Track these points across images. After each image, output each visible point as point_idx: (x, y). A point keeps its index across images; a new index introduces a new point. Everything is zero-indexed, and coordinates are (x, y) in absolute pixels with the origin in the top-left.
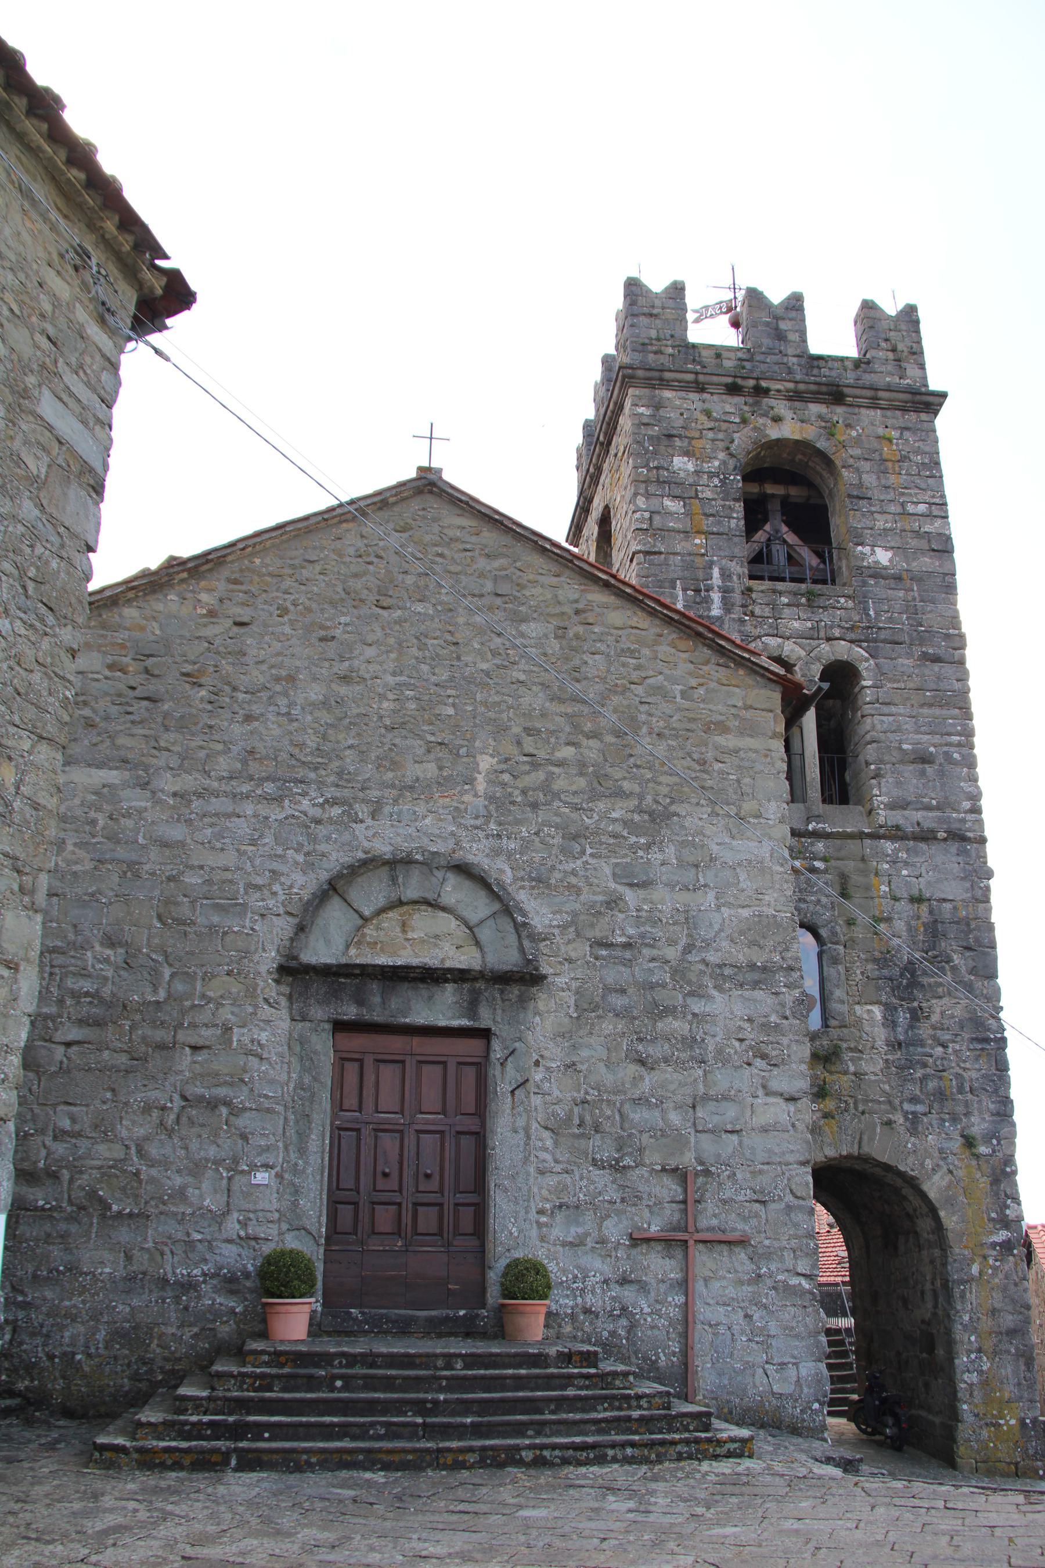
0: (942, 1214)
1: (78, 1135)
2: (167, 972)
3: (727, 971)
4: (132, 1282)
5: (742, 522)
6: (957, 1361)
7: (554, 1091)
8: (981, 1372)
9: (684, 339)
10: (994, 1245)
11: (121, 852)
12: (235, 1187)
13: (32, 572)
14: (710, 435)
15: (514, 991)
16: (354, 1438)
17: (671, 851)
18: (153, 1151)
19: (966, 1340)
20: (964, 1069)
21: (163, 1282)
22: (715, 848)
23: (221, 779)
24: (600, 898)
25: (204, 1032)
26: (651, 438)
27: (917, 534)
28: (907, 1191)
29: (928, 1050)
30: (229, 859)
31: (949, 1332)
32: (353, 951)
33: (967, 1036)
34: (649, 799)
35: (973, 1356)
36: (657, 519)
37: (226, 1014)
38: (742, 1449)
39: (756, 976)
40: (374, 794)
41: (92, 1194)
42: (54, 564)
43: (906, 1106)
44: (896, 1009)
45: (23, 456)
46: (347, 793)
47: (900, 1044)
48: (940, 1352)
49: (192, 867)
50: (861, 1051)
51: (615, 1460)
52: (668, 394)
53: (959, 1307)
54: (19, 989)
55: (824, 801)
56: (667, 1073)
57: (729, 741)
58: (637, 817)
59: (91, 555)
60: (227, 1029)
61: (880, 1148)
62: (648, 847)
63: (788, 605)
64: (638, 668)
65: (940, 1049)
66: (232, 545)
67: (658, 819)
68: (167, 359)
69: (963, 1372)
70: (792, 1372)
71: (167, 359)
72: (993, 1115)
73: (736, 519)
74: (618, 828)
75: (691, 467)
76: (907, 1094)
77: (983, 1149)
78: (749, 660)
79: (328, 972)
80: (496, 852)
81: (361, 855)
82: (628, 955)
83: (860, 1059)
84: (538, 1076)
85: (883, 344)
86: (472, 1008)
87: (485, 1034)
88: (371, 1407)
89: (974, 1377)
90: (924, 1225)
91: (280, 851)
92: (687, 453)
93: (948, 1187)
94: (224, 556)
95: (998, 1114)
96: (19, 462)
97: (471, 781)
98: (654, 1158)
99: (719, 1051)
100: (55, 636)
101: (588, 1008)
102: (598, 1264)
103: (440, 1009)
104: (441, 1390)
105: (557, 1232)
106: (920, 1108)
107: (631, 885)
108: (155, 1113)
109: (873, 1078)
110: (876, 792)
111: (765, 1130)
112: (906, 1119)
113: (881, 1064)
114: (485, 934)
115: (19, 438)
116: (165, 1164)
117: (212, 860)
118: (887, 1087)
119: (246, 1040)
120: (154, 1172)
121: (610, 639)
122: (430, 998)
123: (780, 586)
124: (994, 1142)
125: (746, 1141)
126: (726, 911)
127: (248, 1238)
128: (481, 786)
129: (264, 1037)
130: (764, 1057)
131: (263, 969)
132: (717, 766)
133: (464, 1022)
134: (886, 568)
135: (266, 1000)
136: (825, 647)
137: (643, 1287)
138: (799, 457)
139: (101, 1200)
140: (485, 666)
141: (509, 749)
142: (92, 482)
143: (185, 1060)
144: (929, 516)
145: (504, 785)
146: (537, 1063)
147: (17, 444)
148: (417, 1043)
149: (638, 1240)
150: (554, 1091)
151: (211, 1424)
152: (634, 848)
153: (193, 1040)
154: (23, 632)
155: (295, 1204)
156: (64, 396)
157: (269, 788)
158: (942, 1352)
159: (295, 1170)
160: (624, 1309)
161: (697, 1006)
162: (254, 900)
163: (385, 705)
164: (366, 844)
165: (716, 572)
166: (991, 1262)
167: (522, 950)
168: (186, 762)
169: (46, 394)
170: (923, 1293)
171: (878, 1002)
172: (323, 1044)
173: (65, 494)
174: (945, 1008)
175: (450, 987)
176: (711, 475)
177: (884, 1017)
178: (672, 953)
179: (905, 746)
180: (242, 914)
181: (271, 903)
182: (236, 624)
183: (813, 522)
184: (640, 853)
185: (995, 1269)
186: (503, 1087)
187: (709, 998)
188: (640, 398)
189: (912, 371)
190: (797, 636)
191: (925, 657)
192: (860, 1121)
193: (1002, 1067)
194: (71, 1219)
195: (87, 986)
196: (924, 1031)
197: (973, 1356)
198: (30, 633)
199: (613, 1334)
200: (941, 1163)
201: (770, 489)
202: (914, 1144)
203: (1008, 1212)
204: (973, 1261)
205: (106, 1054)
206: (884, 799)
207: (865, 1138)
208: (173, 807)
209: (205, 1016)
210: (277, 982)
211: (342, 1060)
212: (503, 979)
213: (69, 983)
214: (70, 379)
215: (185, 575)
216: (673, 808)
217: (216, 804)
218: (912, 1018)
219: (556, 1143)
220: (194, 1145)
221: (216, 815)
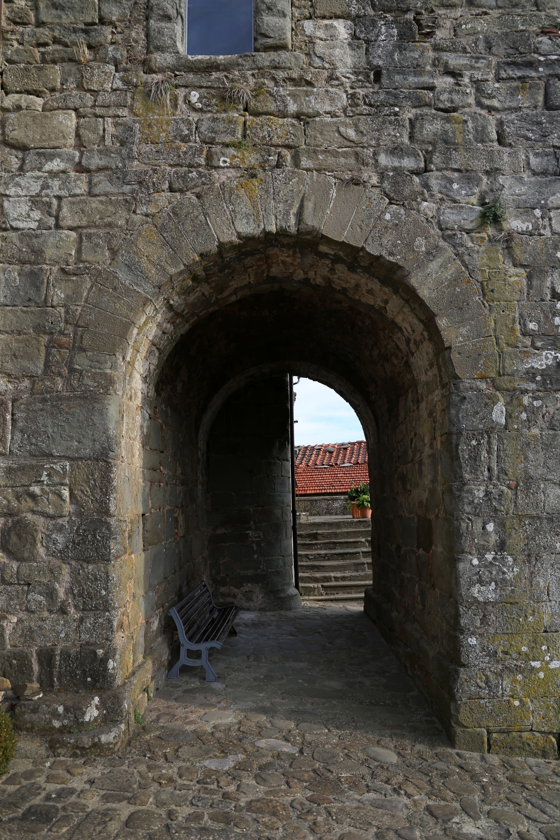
0: (442, 322)
8: (501, 583)
20: (490, 109)
29: (426, 79)
31: (452, 518)
33: (494, 60)
35: (489, 557)
43: (383, 160)
44: (374, 23)
47: (378, 75)
48: (439, 548)
50: (309, 84)
53: (467, 476)
65: (450, 80)
69: (471, 584)
72: (535, 173)
76: (385, 141)
83: (307, 94)
95: (544, 173)
106: (408, 163)
109: (328, 119)
112: (382, 176)
113: (344, 100)
118: (351, 133)
158: (440, 549)
166: (526, 400)
170: (421, 463)
177: (354, 36)
185: (532, 411)
192: (301, 181)
197: (489, 557)
200: (442, 243)
202: (395, 215)
207: (309, 206)
218: (401, 36)
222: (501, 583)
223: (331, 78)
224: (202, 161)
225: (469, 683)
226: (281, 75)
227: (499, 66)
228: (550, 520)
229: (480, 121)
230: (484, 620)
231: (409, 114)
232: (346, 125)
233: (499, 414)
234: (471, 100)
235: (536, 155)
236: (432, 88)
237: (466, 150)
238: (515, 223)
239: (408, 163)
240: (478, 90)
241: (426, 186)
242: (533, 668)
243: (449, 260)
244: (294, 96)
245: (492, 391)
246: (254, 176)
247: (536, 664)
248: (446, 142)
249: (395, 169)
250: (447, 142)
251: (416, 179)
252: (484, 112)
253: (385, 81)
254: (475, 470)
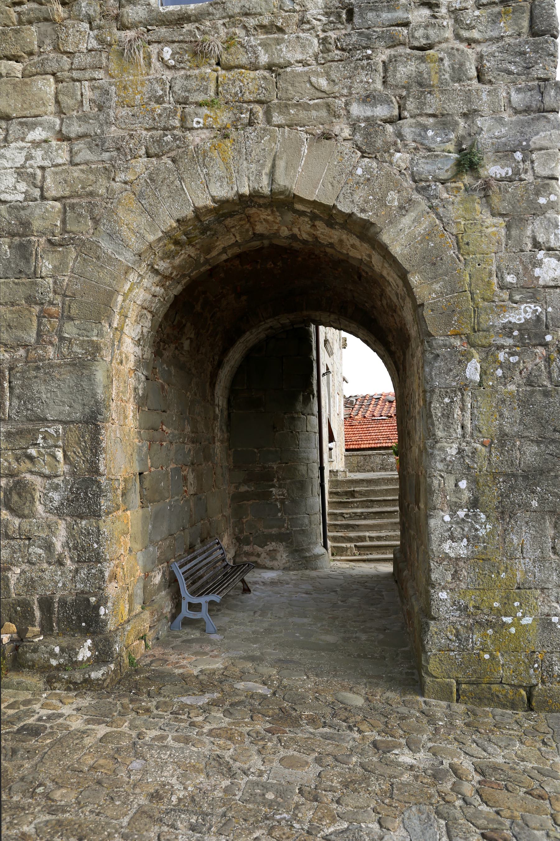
0: (415, 279)
6: (432, 522)
8: (473, 540)
10: (508, 330)
20: (470, 42)
29: (400, 15)
35: (461, 514)
43: (356, 110)
50: (280, 30)
53: (440, 434)
65: (426, 12)
69: (443, 540)
72: (517, 112)
76: (358, 89)
77: (494, 170)
83: (278, 42)
89: (461, 549)
95: (527, 110)
106: (381, 111)
109: (299, 69)
112: (354, 127)
118: (323, 83)
124: (518, 156)
192: (273, 139)
197: (461, 514)
200: (416, 196)
202: (367, 170)
203: (537, 272)
204: (468, 357)
207: (281, 164)
223: (302, 21)
224: (177, 123)
226: (252, 22)
228: (526, 477)
229: (458, 56)
230: (455, 575)
231: (383, 55)
232: (318, 75)
233: (473, 370)
234: (449, 34)
235: (519, 90)
236: (406, 24)
237: (442, 92)
238: (494, 170)
239: (381, 111)
240: (457, 21)
241: (400, 135)
242: (504, 623)
243: (423, 214)
244: (264, 44)
245: (466, 347)
246: (226, 136)
247: (508, 620)
248: (421, 85)
249: (367, 119)
250: (422, 83)
251: (390, 128)
252: (463, 46)
253: (357, 20)
254: (447, 427)
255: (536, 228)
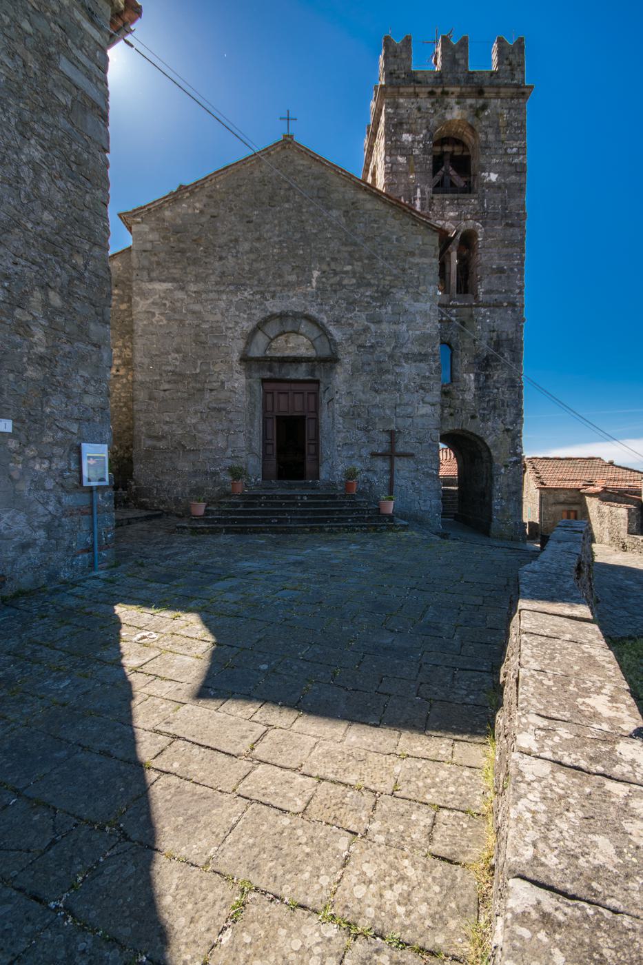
0: (492, 450)
1: (173, 423)
2: (199, 362)
3: (410, 356)
4: (195, 473)
5: (431, 166)
7: (343, 402)
9: (410, 69)
10: (510, 462)
11: (177, 316)
12: (229, 439)
13: (73, 158)
14: (420, 121)
15: (328, 364)
16: (266, 523)
17: (389, 308)
18: (200, 427)
19: (497, 495)
21: (206, 473)
22: (407, 306)
23: (212, 285)
24: (361, 328)
25: (215, 384)
26: (393, 125)
27: (511, 164)
28: (479, 442)
30: (219, 317)
31: (491, 492)
32: (268, 352)
34: (381, 287)
36: (394, 167)
37: (222, 377)
38: (405, 528)
39: (421, 358)
40: (272, 289)
41: (179, 443)
42: (85, 156)
43: (481, 411)
45: (55, 92)
46: (262, 289)
48: (487, 498)
49: (204, 321)
51: (358, 531)
52: (401, 100)
54: (102, 356)
55: (457, 292)
56: (385, 395)
57: (416, 260)
58: (376, 295)
59: (107, 155)
60: (223, 383)
61: (471, 426)
62: (380, 307)
63: (449, 205)
64: (378, 228)
66: (206, 178)
67: (384, 295)
68: (132, 46)
70: (428, 503)
71: (132, 46)
73: (429, 166)
74: (369, 300)
75: (410, 139)
78: (425, 222)
79: (257, 360)
80: (320, 311)
81: (268, 314)
82: (371, 350)
84: (337, 397)
85: (505, 62)
86: (312, 372)
87: (317, 382)
88: (273, 512)
89: (499, 507)
90: (485, 455)
91: (237, 313)
92: (409, 132)
93: (495, 441)
94: (203, 184)
96: (53, 96)
97: (310, 282)
98: (380, 426)
99: (406, 387)
100: (92, 193)
101: (356, 370)
102: (359, 464)
103: (301, 373)
104: (298, 507)
105: (344, 453)
106: (486, 412)
107: (373, 323)
108: (199, 414)
110: (479, 287)
111: (422, 416)
114: (317, 343)
115: (51, 81)
116: (204, 432)
117: (212, 318)
119: (230, 386)
120: (200, 435)
121: (367, 216)
122: (297, 369)
123: (446, 196)
125: (415, 421)
126: (410, 332)
127: (235, 457)
128: (314, 284)
129: (236, 385)
130: (423, 389)
131: (234, 360)
132: (409, 271)
133: (310, 378)
134: (494, 183)
135: (236, 371)
136: (463, 224)
137: (375, 473)
138: (460, 129)
139: (182, 445)
140: (315, 231)
141: (325, 267)
142: (100, 113)
143: (207, 395)
144: (518, 154)
145: (323, 283)
146: (337, 392)
147: (50, 86)
148: (293, 386)
149: (374, 455)
150: (343, 402)
151: (216, 519)
152: (375, 307)
153: (209, 387)
154: (73, 189)
155: (251, 445)
156: (75, 62)
157: (232, 288)
159: (250, 432)
160: (368, 480)
161: (397, 370)
162: (229, 334)
163: (275, 251)
164: (270, 309)
165: (419, 190)
167: (331, 349)
168: (198, 278)
169: (63, 58)
171: (473, 373)
172: (257, 387)
173: (85, 119)
174: (499, 375)
175: (304, 364)
176: (419, 142)
178: (388, 349)
179: (494, 267)
180: (225, 339)
181: (236, 334)
182: (212, 217)
183: (463, 164)
184: (377, 309)
185: (510, 470)
186: (324, 401)
187: (403, 367)
188: (388, 104)
189: (518, 76)
190: (450, 219)
191: (507, 224)
193: (520, 396)
194: (172, 452)
195: (169, 368)
196: (490, 382)
198: (78, 190)
199: (364, 488)
201: (447, 149)
205: (179, 394)
206: (482, 290)
208: (195, 298)
209: (214, 378)
210: (240, 364)
211: (266, 393)
212: (323, 360)
213: (163, 368)
214: (75, 51)
215: (188, 194)
216: (391, 290)
217: (212, 295)
219: (344, 422)
220: (214, 425)
221: (212, 300)
222: (502, 506)
225: (494, 525)
227: (509, 387)
233: (503, 470)
255: (517, 440)
